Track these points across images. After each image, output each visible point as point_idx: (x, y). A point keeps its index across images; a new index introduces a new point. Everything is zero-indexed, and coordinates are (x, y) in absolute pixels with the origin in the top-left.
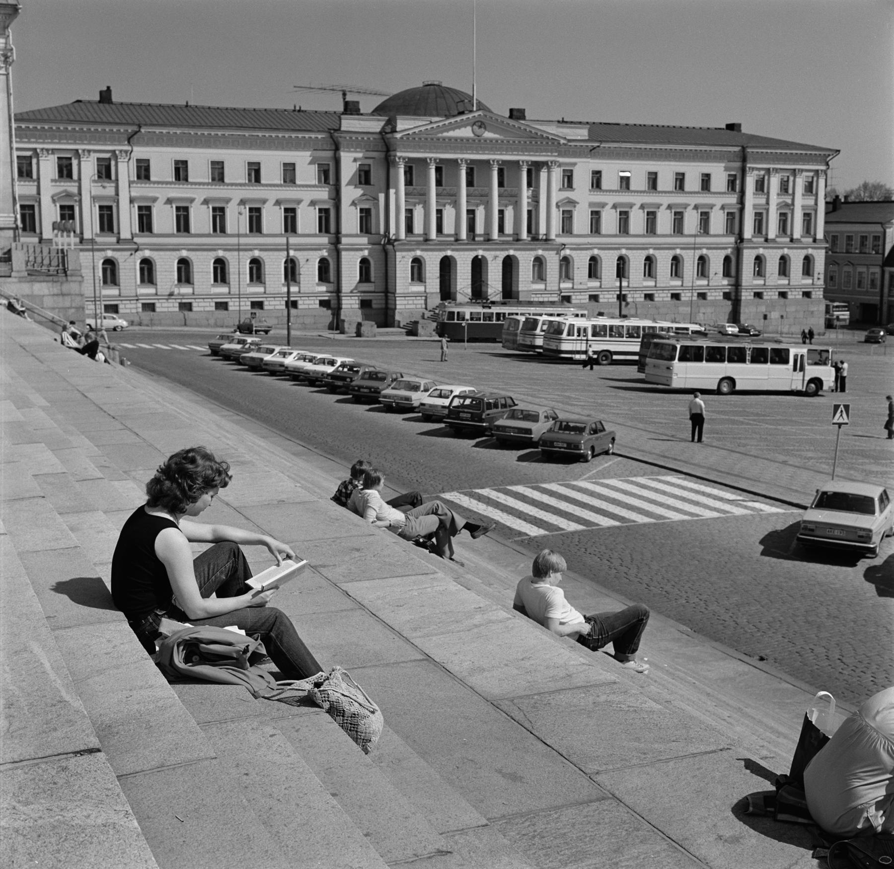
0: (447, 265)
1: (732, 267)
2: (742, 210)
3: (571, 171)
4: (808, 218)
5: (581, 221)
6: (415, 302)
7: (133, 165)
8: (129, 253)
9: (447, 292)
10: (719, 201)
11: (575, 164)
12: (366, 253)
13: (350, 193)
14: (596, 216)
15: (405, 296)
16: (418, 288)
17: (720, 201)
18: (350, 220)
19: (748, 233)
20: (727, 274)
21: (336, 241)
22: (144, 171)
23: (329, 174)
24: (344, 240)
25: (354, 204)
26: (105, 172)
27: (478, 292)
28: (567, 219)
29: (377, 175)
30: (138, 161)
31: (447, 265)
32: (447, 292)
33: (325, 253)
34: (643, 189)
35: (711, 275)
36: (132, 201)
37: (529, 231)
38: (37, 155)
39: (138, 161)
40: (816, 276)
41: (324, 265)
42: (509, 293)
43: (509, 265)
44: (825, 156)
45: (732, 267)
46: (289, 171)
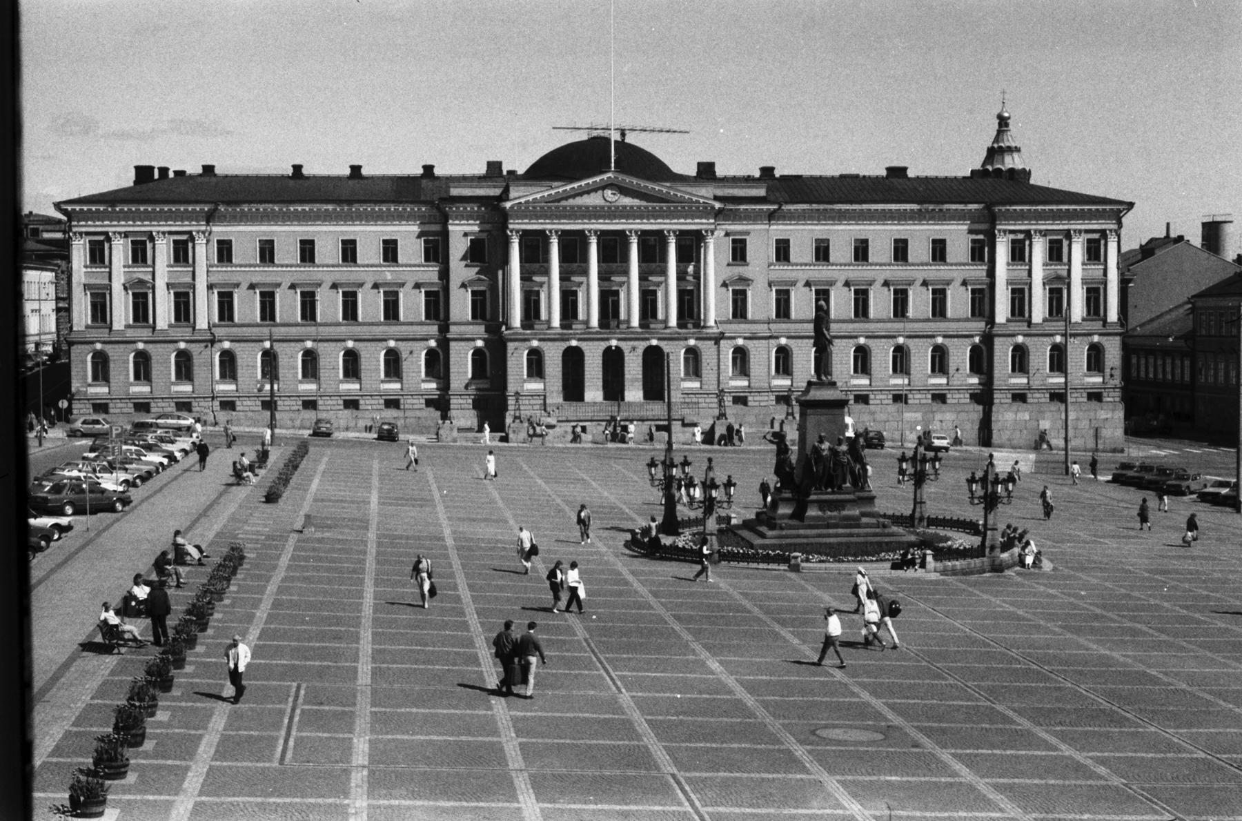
0: (573, 360)
2: (992, 286)
6: (532, 402)
8: (203, 345)
10: (957, 274)
11: (748, 233)
12: (480, 343)
13: (460, 271)
16: (535, 386)
18: (461, 305)
21: (444, 328)
22: (225, 251)
23: (436, 250)
24: (453, 329)
25: (463, 286)
26: (182, 253)
30: (219, 242)
31: (573, 360)
33: (433, 343)
34: (848, 261)
35: (952, 370)
36: (210, 287)
38: (109, 240)
39: (219, 242)
40: (1108, 371)
41: (431, 356)
44: (1117, 210)
46: (390, 251)
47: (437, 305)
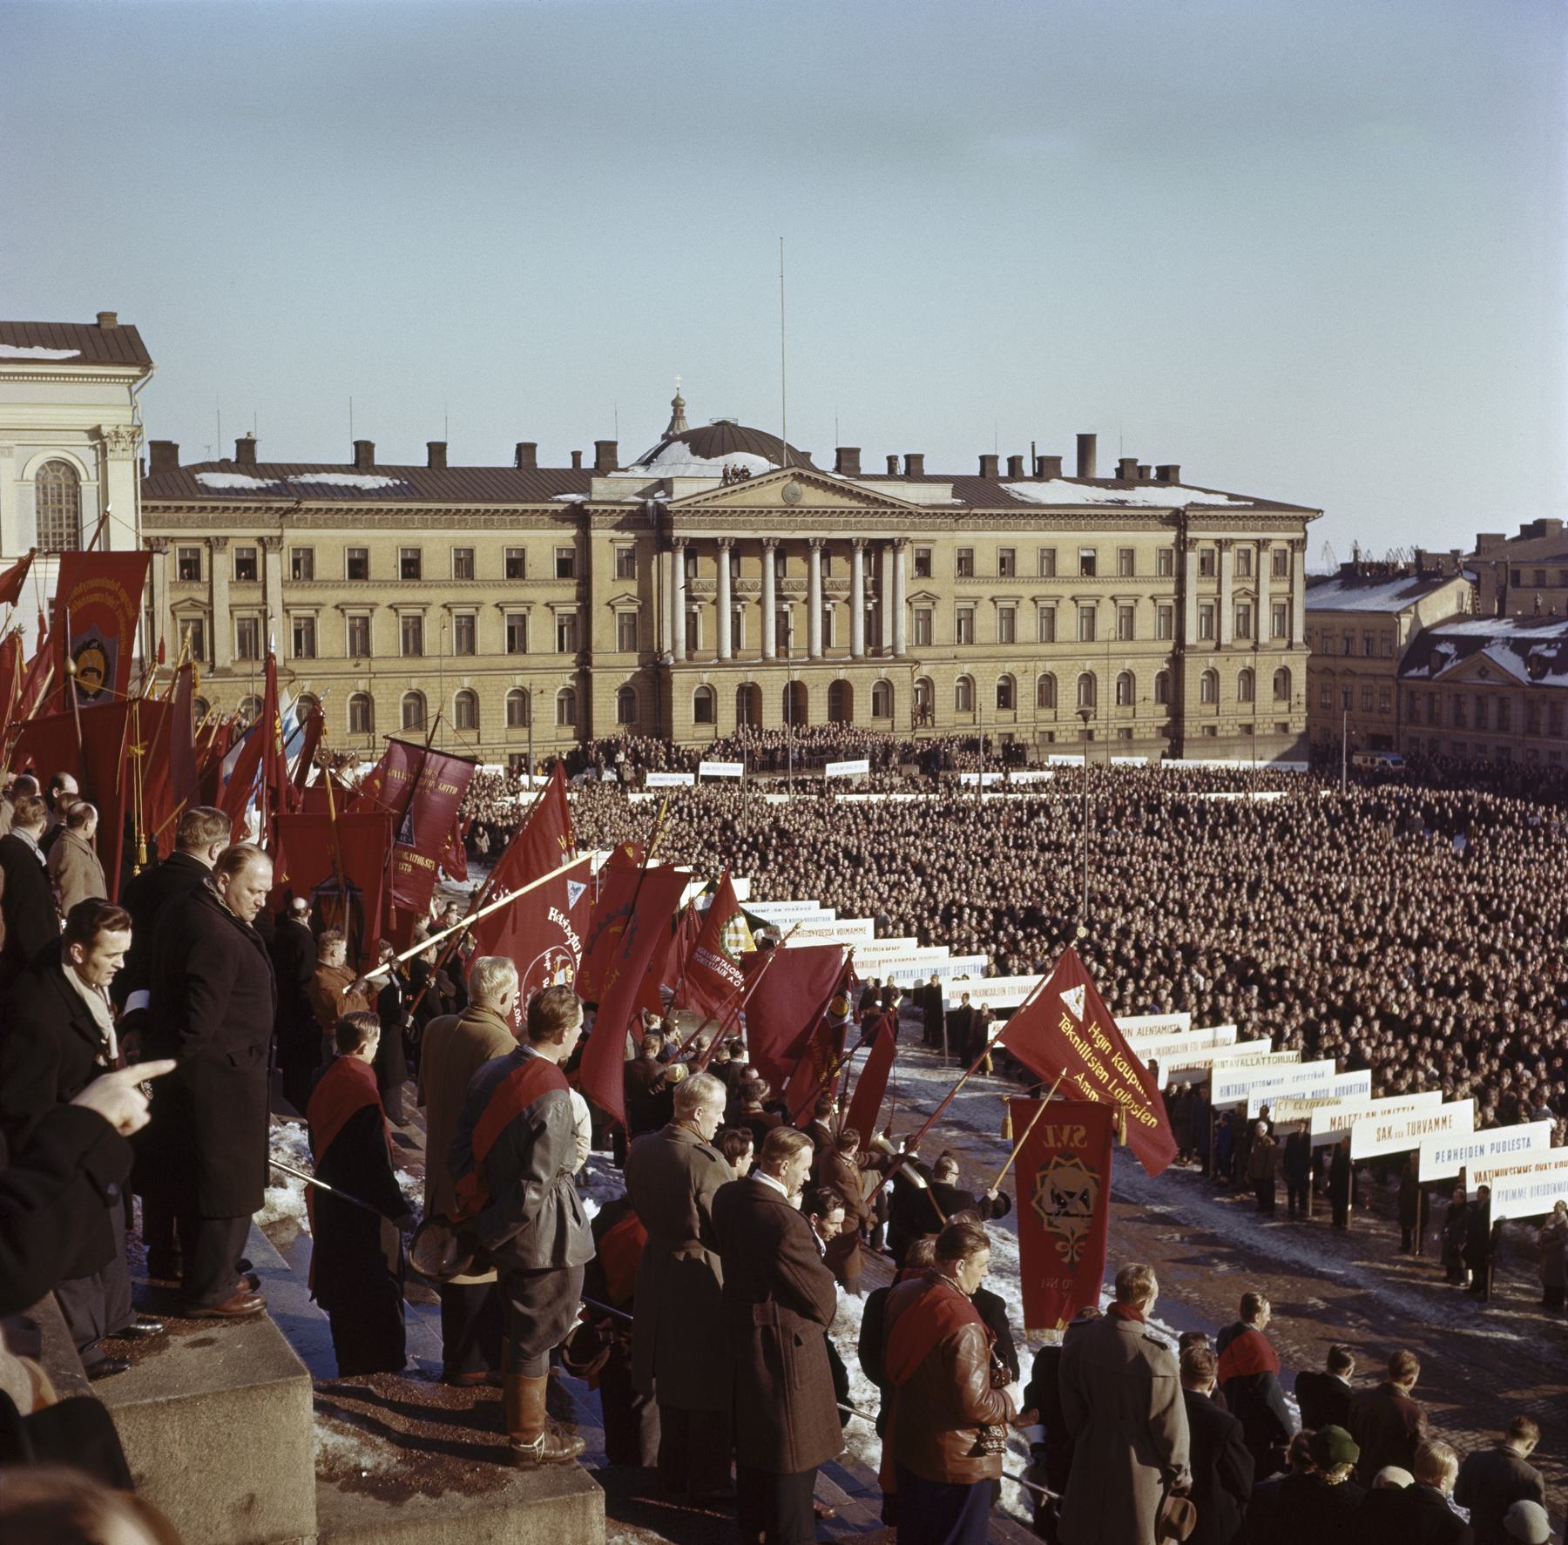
0: (749, 698)
1: (1171, 687)
3: (929, 551)
4: (1283, 613)
7: (287, 557)
10: (1147, 590)
11: (932, 541)
17: (1153, 588)
18: (605, 630)
19: (1191, 638)
20: (1162, 697)
22: (303, 564)
26: (247, 568)
28: (925, 620)
37: (868, 641)
40: (1294, 700)
45: (1171, 687)
47: (577, 633)
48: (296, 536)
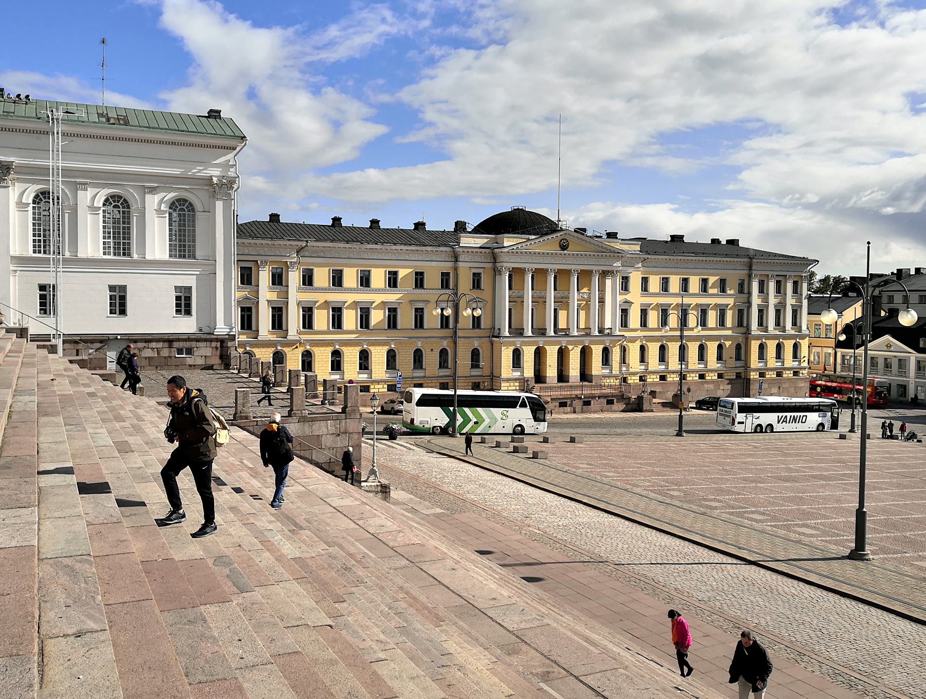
0: (539, 354)
5: (634, 319)
9: (539, 377)
14: (644, 312)
15: (508, 380)
16: (517, 374)
24: (460, 333)
26: (278, 279)
27: (562, 377)
29: (485, 282)
32: (539, 377)
42: (585, 376)
43: (585, 354)
48: (307, 262)
